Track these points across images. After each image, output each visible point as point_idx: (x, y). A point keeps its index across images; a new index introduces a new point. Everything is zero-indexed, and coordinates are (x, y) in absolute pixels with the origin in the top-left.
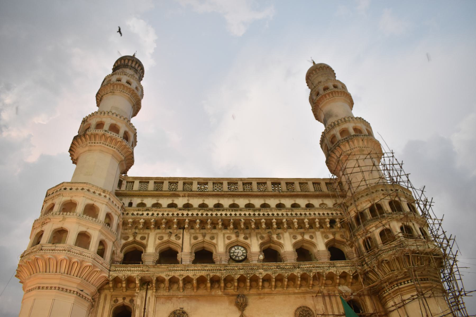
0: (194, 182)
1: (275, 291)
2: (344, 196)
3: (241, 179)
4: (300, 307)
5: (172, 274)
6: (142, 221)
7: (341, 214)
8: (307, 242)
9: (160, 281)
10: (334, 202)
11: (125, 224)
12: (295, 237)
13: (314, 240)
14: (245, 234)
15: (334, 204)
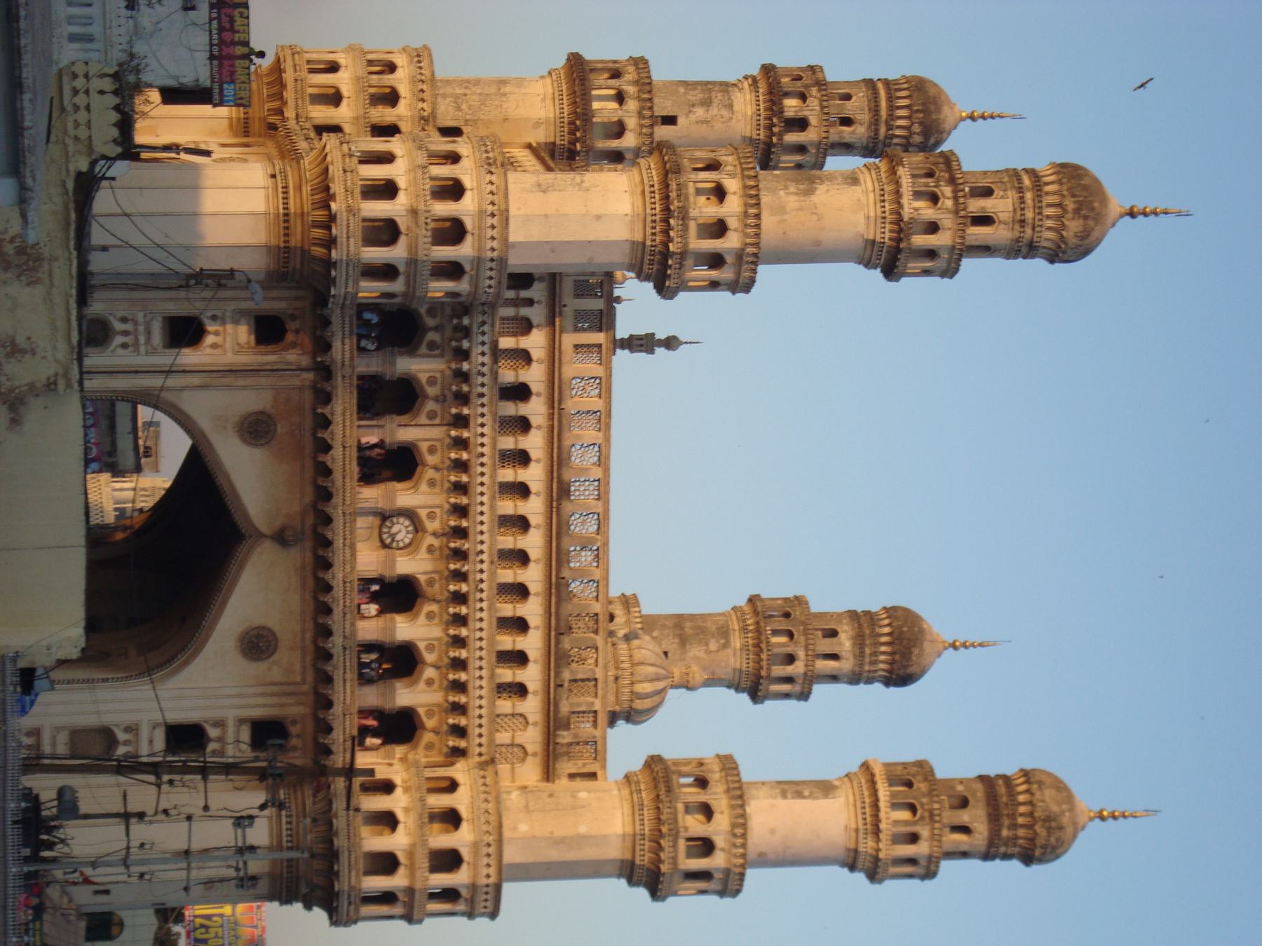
0: (601, 435)
1: (308, 596)
2: (548, 774)
3: (606, 544)
4: (276, 638)
5: (338, 419)
6: (465, 344)
7: (480, 755)
8: (421, 672)
9: (326, 398)
10: (530, 748)
11: (461, 306)
12: (430, 648)
13: (422, 685)
14: (441, 548)
15: (523, 748)
